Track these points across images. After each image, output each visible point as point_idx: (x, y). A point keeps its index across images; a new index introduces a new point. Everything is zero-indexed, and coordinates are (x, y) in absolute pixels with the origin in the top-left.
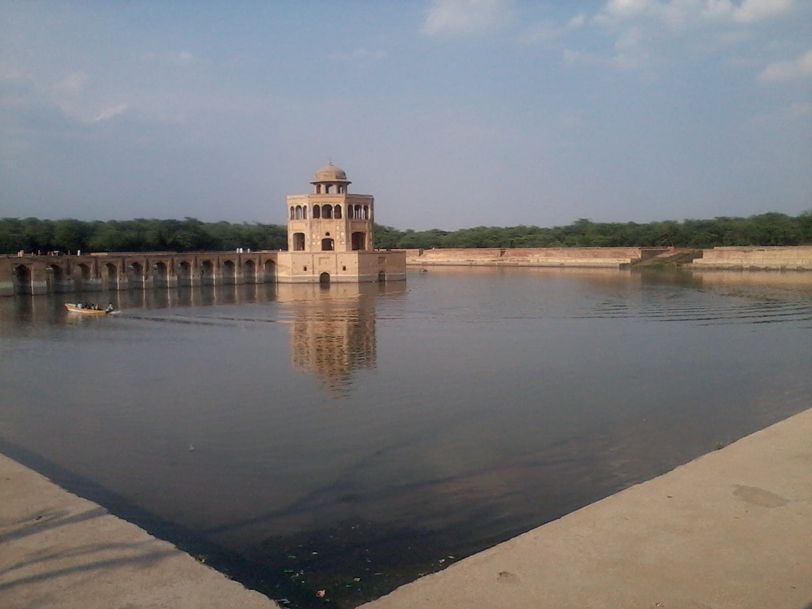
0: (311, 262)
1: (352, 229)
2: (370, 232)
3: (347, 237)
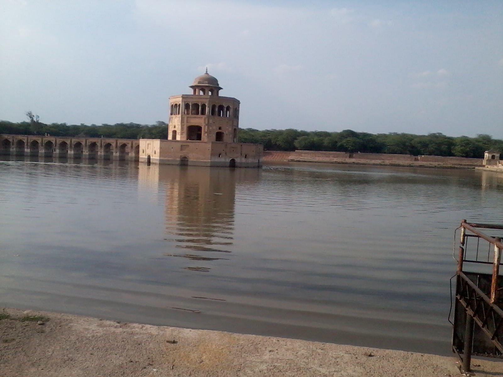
1: (187, 122)
2: (204, 126)
3: (182, 129)
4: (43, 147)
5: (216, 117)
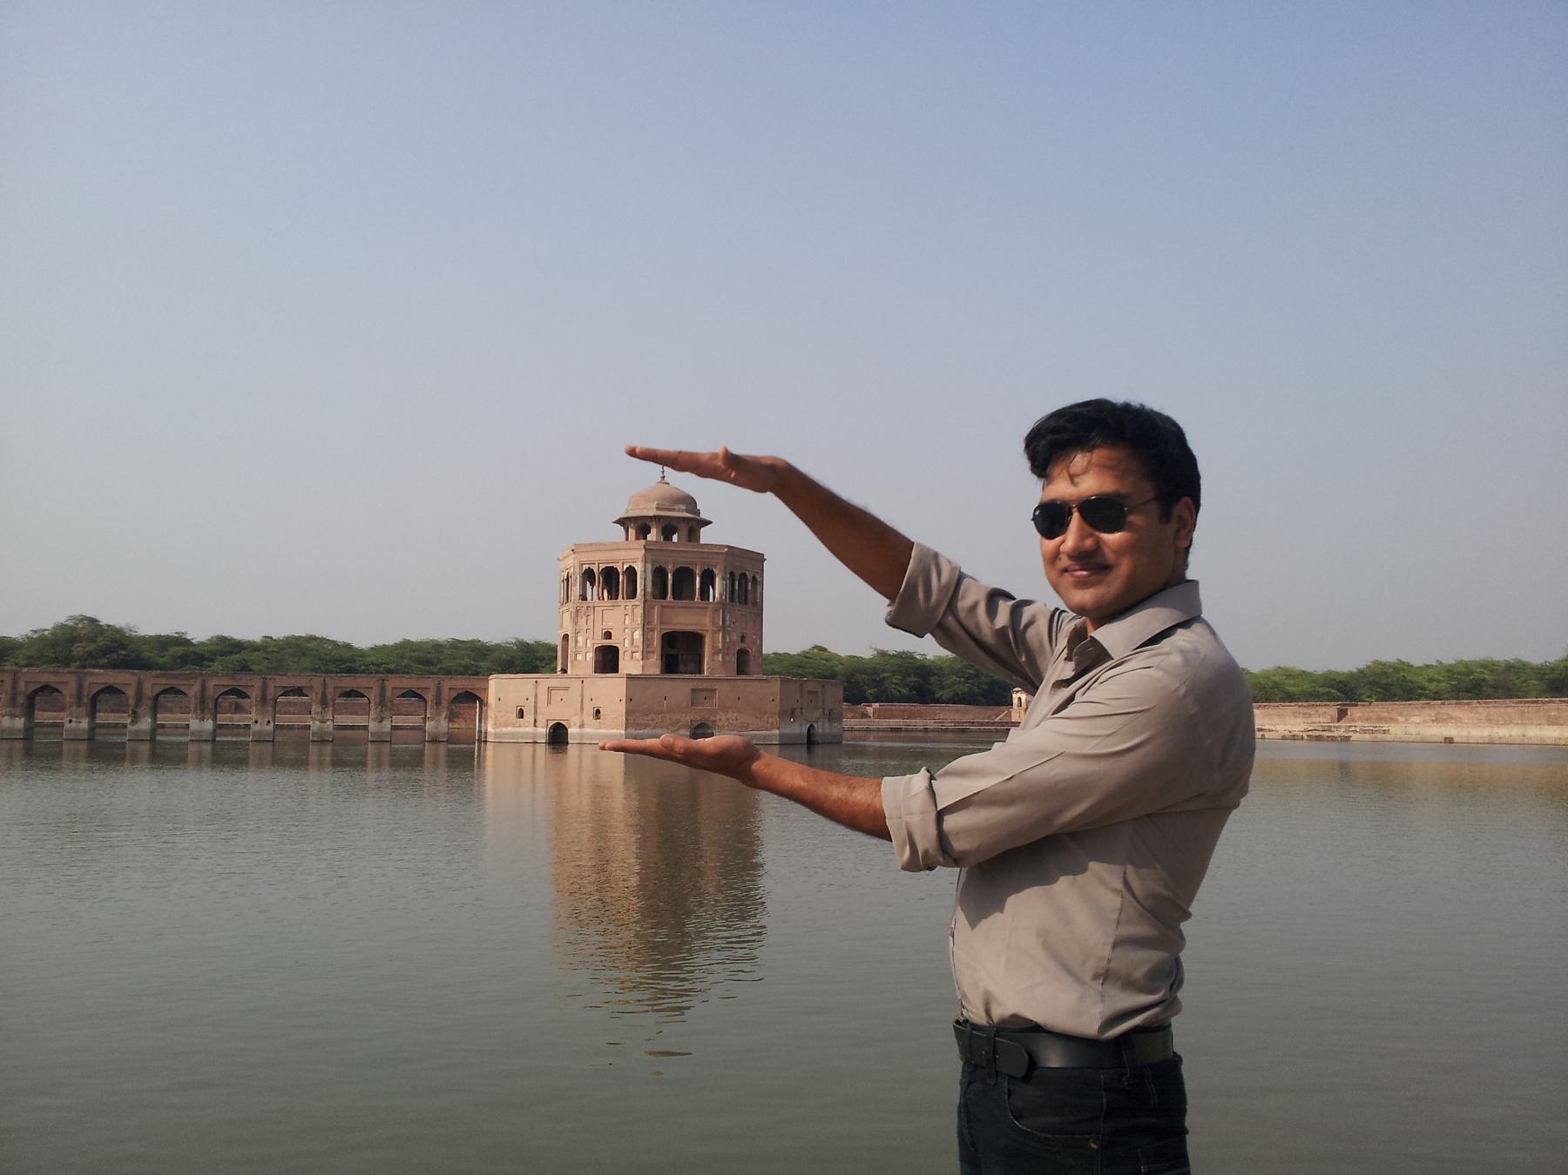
0: (532, 700)
2: (715, 632)
3: (646, 640)
4: (17, 711)
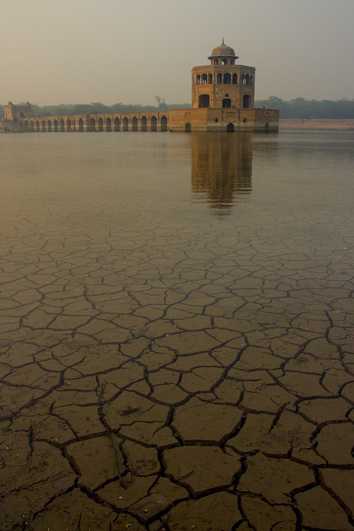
5: (223, 86)
